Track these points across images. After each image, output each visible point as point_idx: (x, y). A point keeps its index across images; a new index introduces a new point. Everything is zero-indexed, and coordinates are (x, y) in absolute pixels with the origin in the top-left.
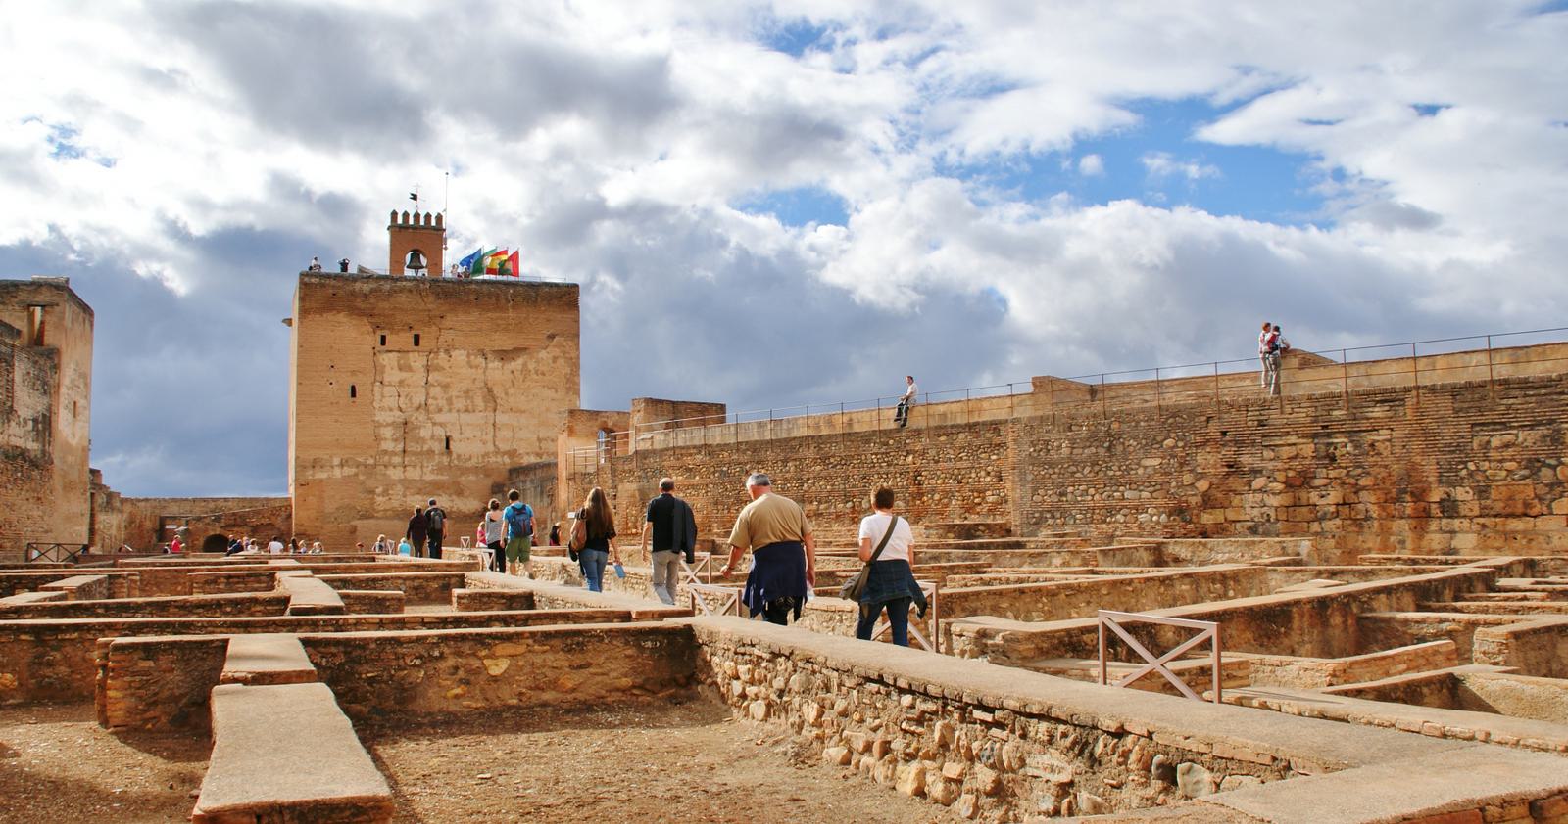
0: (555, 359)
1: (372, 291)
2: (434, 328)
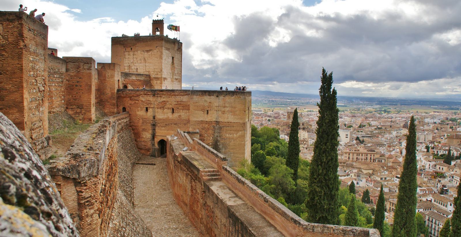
0: (157, 52)
1: (124, 40)
2: (135, 47)
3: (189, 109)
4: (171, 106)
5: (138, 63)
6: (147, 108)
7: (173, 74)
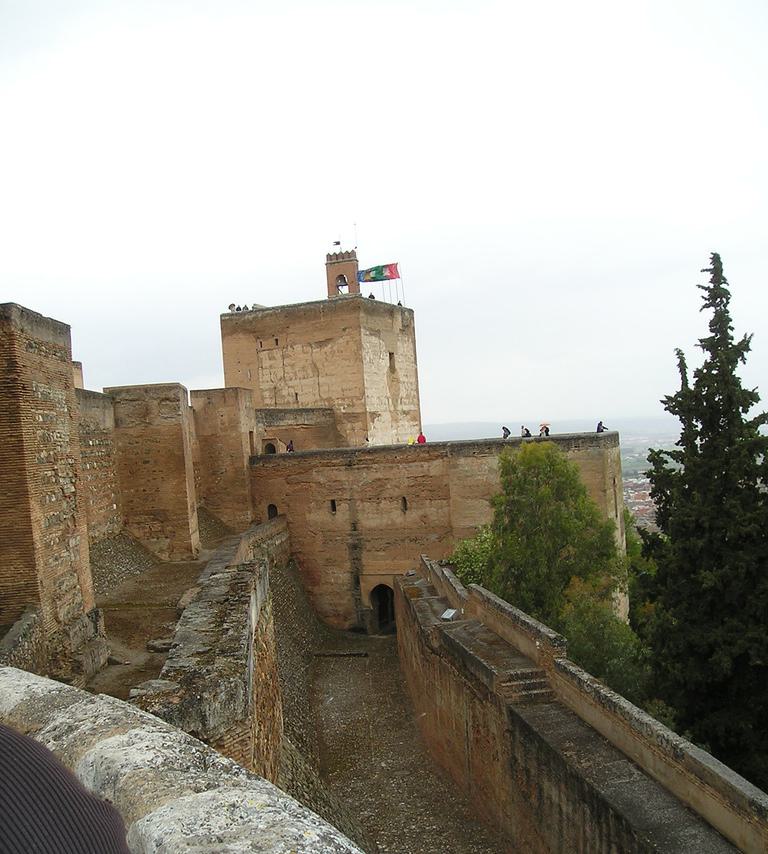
3: (447, 497)
4: (397, 492)
5: (298, 379)
6: (333, 502)
7: (396, 398)
